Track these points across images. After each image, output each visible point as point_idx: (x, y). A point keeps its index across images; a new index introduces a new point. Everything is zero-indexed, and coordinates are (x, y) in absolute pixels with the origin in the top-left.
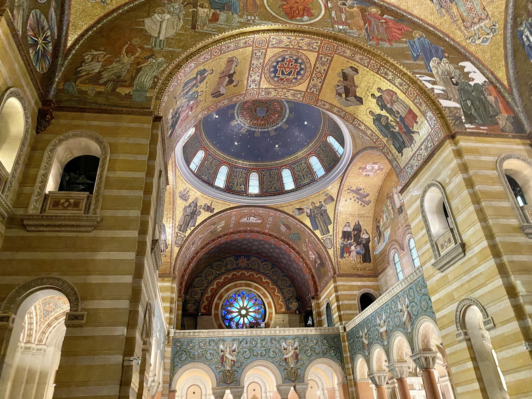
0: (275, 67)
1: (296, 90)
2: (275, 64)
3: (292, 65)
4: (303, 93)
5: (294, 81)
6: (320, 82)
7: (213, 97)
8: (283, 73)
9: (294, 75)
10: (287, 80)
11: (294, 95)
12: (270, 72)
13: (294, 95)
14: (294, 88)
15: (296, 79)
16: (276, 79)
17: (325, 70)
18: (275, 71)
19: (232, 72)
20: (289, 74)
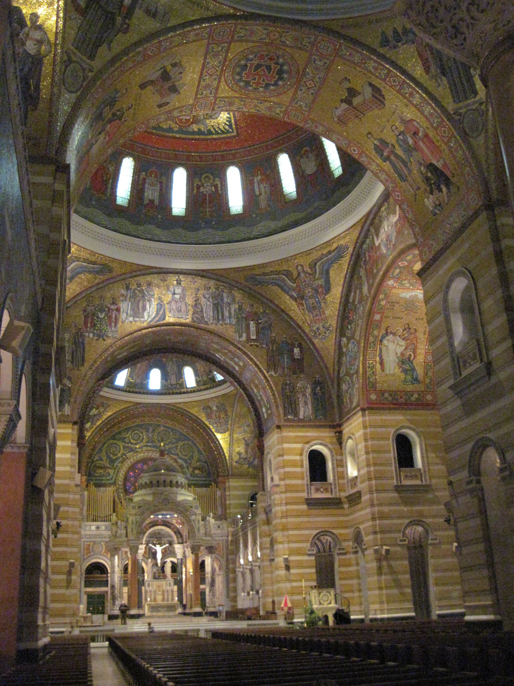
0: (281, 78)
1: (248, 41)
2: (280, 83)
3: (255, 79)
4: (235, 38)
5: (251, 57)
6: (208, 63)
7: (384, 98)
8: (269, 68)
9: (252, 65)
10: (262, 57)
11: (252, 33)
12: (289, 72)
13: (252, 33)
14: (251, 45)
15: (248, 60)
16: (281, 60)
17: (204, 80)
18: (280, 72)
19: (344, 106)
20: (258, 66)
